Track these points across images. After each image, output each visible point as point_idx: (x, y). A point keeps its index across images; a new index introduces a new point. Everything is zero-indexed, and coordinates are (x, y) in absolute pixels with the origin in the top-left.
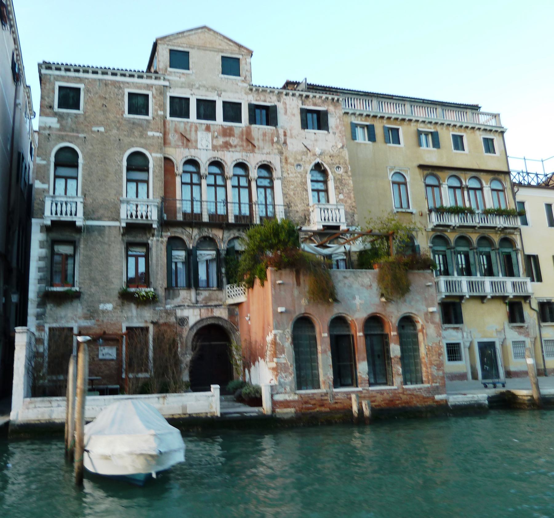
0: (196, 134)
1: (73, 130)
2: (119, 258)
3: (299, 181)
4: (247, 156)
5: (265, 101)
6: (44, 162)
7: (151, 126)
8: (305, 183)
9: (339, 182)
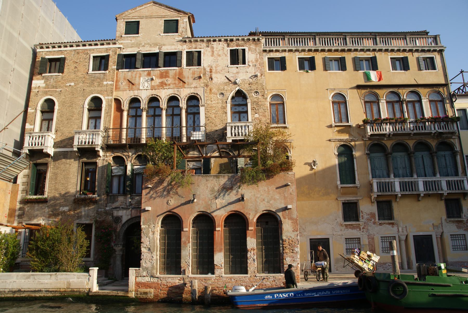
0: (140, 79)
1: (53, 87)
3: (220, 106)
4: (178, 91)
5: (196, 48)
6: (33, 111)
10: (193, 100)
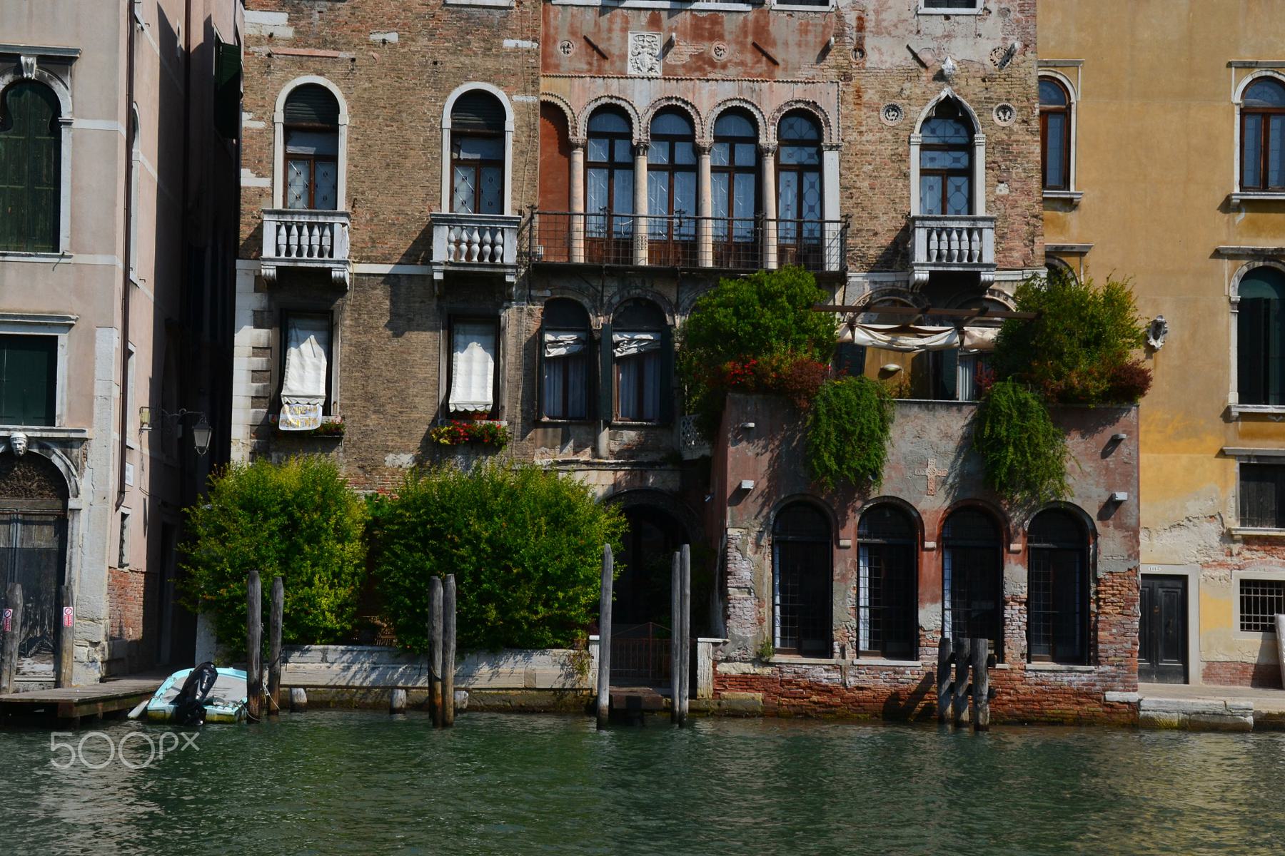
0: (625, 40)
1: (324, 44)
2: (430, 351)
3: (889, 152)
4: (753, 91)
6: (261, 125)
7: (514, 24)
8: (903, 158)
9: (1002, 147)
10: (804, 126)
